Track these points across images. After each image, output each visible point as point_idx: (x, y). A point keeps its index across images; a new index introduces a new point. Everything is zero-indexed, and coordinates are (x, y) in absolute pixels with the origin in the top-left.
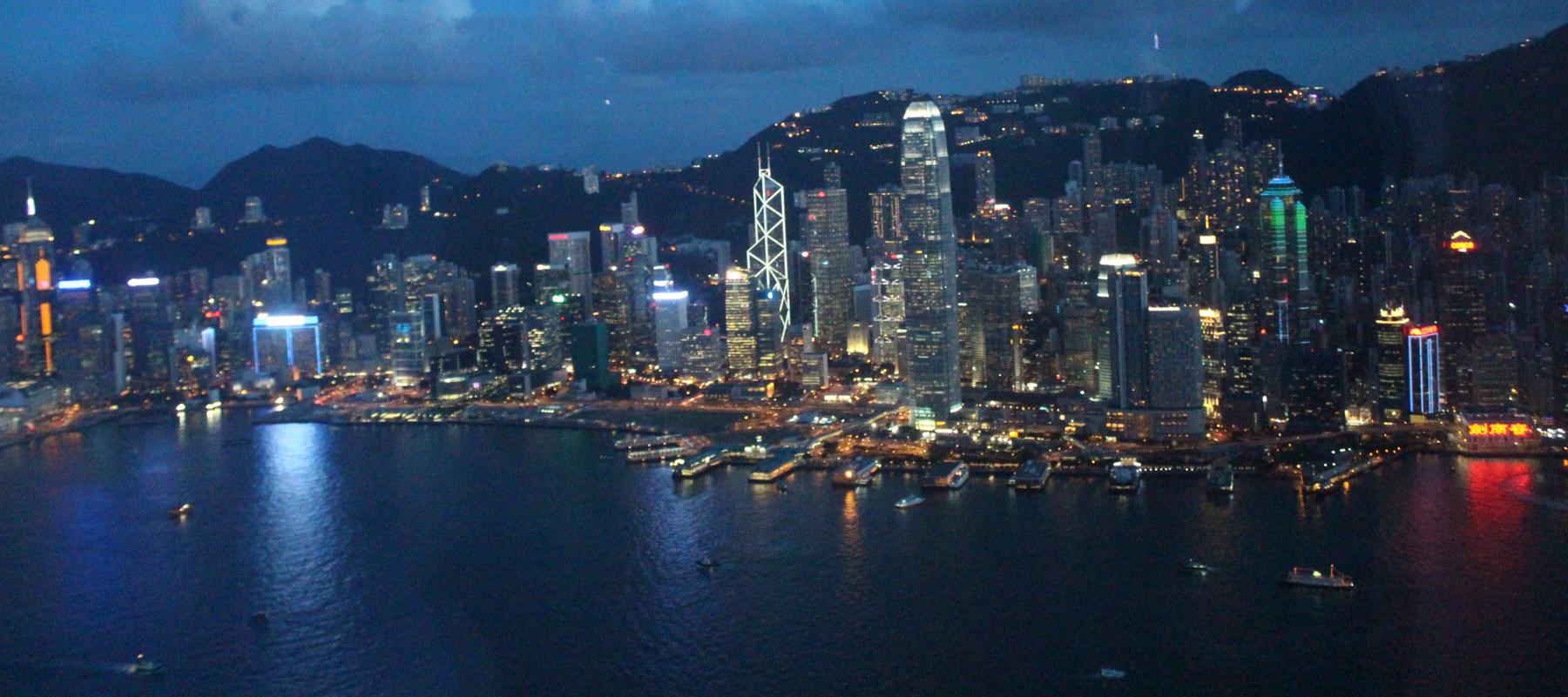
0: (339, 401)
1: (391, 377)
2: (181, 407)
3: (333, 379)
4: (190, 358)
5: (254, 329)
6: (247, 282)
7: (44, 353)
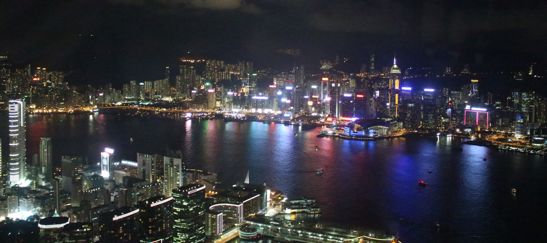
0: (494, 140)
1: (514, 134)
2: (438, 134)
3: (492, 132)
4: (442, 118)
5: (465, 111)
6: (463, 95)
7: (396, 110)
